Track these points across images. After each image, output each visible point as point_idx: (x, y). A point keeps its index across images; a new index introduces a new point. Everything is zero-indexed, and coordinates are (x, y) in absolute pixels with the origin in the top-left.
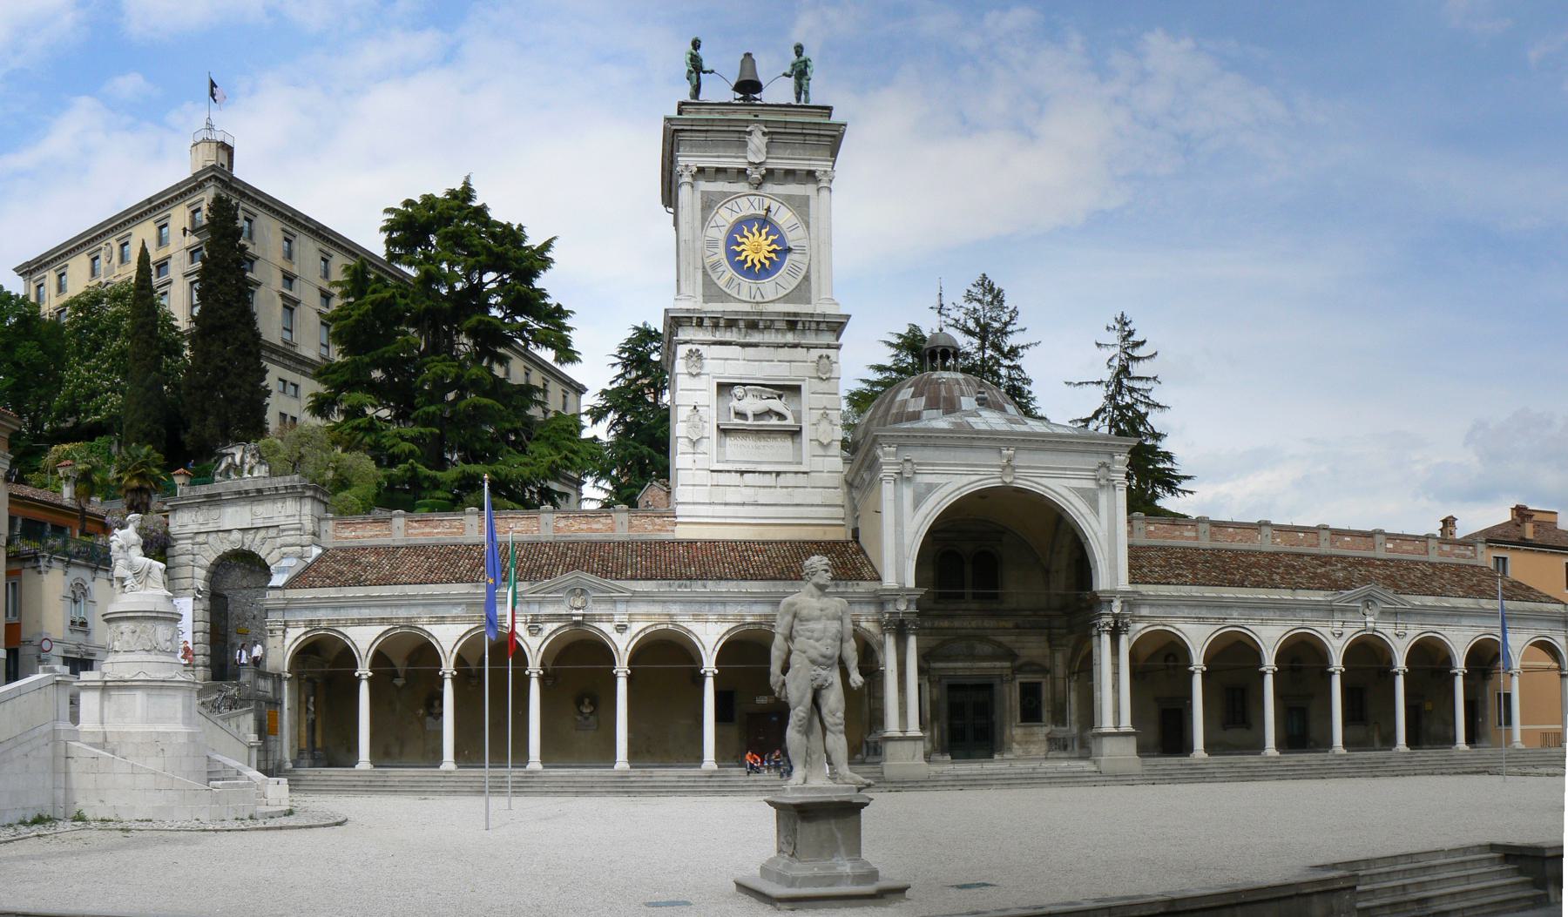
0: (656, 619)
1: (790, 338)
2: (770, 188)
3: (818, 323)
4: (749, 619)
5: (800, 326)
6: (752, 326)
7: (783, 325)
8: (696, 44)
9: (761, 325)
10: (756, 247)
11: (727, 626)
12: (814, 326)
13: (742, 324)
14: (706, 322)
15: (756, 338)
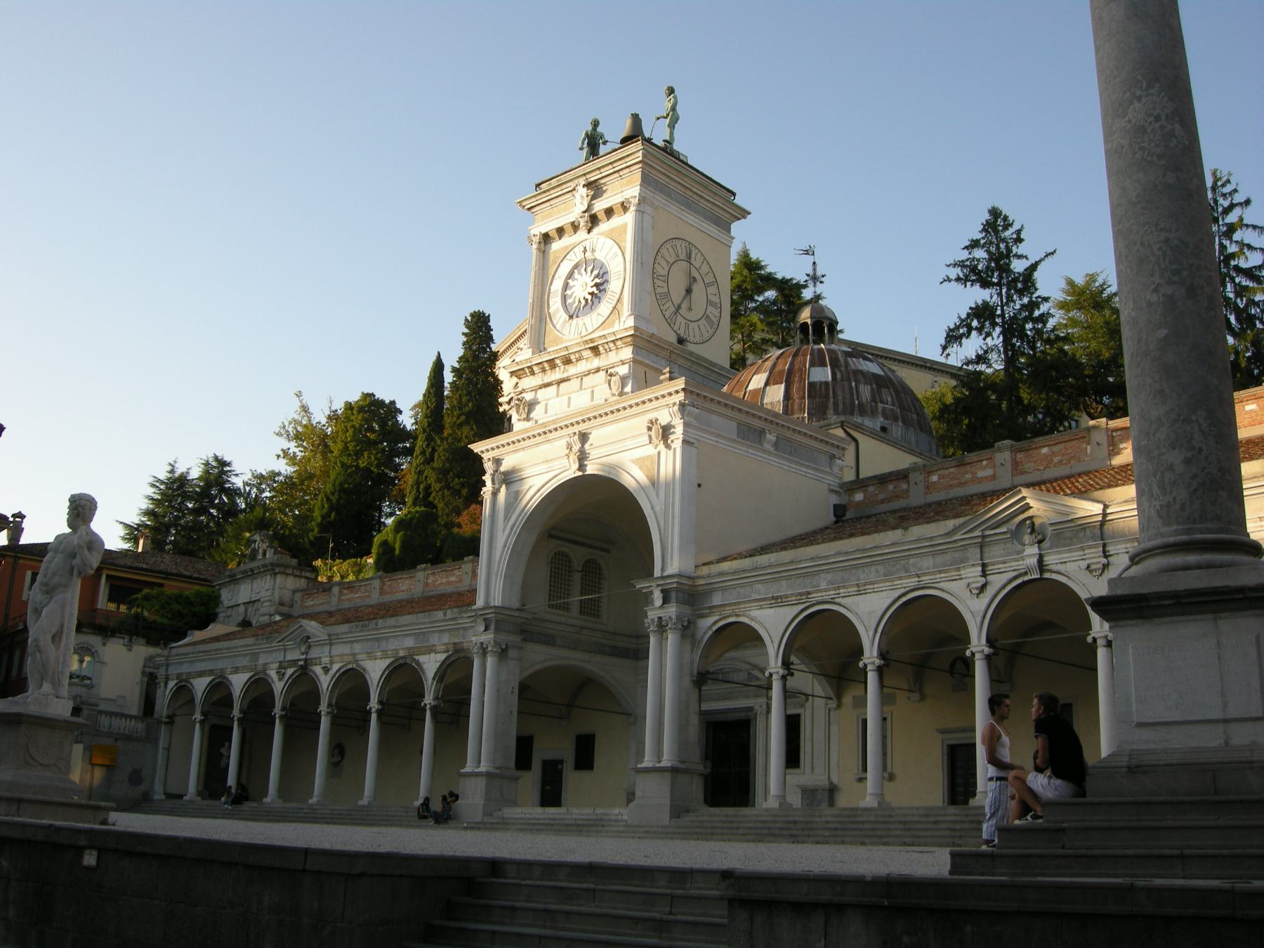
0: (347, 659)
1: (596, 362)
2: (604, 226)
3: (613, 341)
4: (401, 654)
5: (601, 348)
6: (567, 361)
7: (587, 354)
8: (596, 124)
9: (572, 357)
10: (582, 286)
11: (388, 661)
12: (611, 345)
13: (558, 362)
14: (535, 368)
15: (572, 370)
